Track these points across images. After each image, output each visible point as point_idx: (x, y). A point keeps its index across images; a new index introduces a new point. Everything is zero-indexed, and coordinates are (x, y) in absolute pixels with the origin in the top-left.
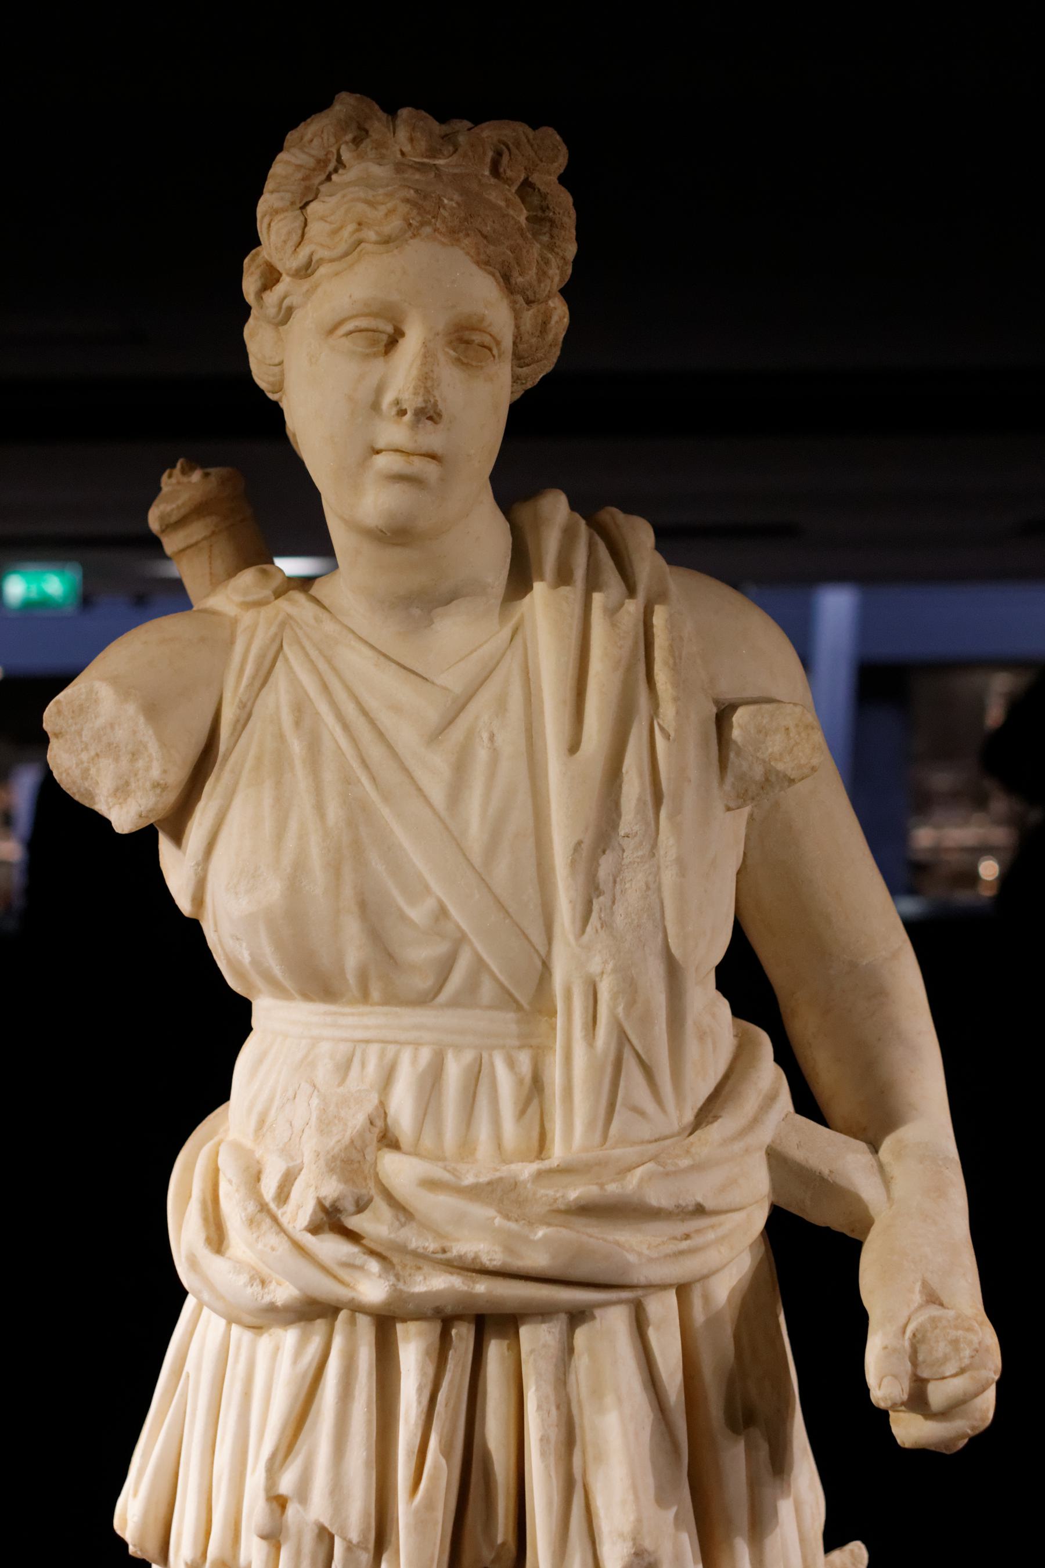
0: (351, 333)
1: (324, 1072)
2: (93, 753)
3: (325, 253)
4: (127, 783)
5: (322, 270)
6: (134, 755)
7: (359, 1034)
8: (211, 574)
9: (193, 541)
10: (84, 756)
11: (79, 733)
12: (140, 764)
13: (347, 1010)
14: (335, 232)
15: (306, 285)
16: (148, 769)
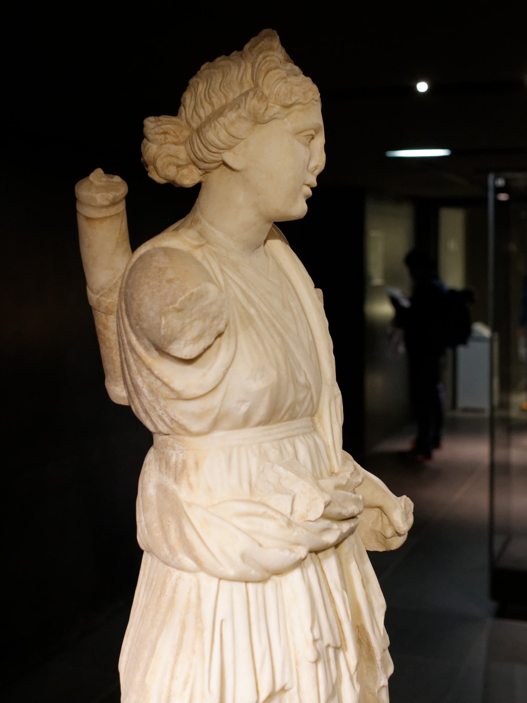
0: (305, 136)
1: (273, 454)
2: (193, 318)
3: (301, 100)
4: (204, 332)
5: (297, 107)
6: (214, 318)
7: (280, 436)
8: (120, 229)
9: (119, 212)
10: (188, 321)
11: (192, 309)
12: (216, 322)
13: (273, 426)
14: (304, 93)
15: (287, 111)
16: (218, 324)
